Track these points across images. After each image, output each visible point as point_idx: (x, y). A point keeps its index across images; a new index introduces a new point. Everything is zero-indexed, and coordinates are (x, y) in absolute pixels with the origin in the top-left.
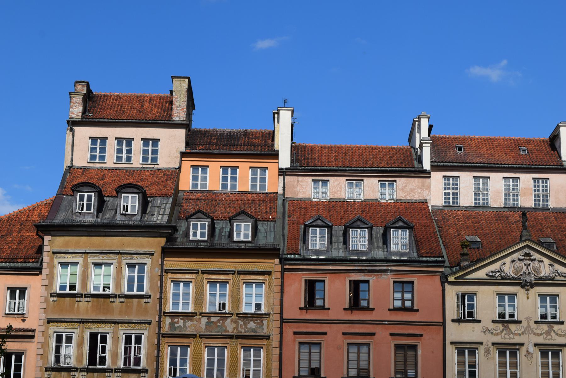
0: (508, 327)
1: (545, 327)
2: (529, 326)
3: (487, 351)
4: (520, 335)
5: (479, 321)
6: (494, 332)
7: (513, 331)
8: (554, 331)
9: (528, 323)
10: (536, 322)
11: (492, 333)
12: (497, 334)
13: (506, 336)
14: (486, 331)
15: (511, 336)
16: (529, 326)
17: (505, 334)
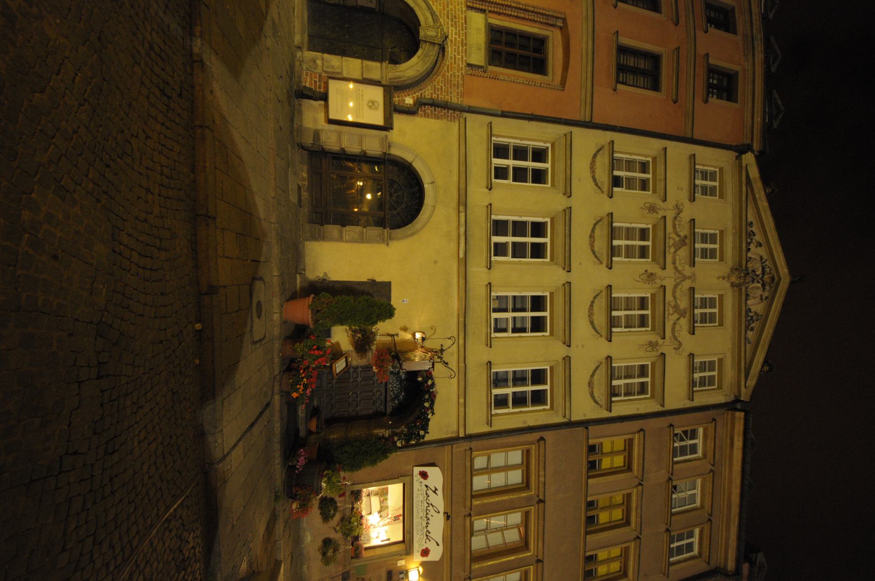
0: (683, 245)
1: (684, 304)
2: (685, 278)
3: (652, 209)
4: (674, 263)
5: (692, 199)
6: (677, 223)
7: (679, 252)
8: (678, 319)
9: (689, 278)
10: (692, 290)
11: (675, 218)
12: (674, 227)
13: (672, 241)
14: (679, 210)
15: (672, 250)
16: (685, 278)
17: (674, 239)
